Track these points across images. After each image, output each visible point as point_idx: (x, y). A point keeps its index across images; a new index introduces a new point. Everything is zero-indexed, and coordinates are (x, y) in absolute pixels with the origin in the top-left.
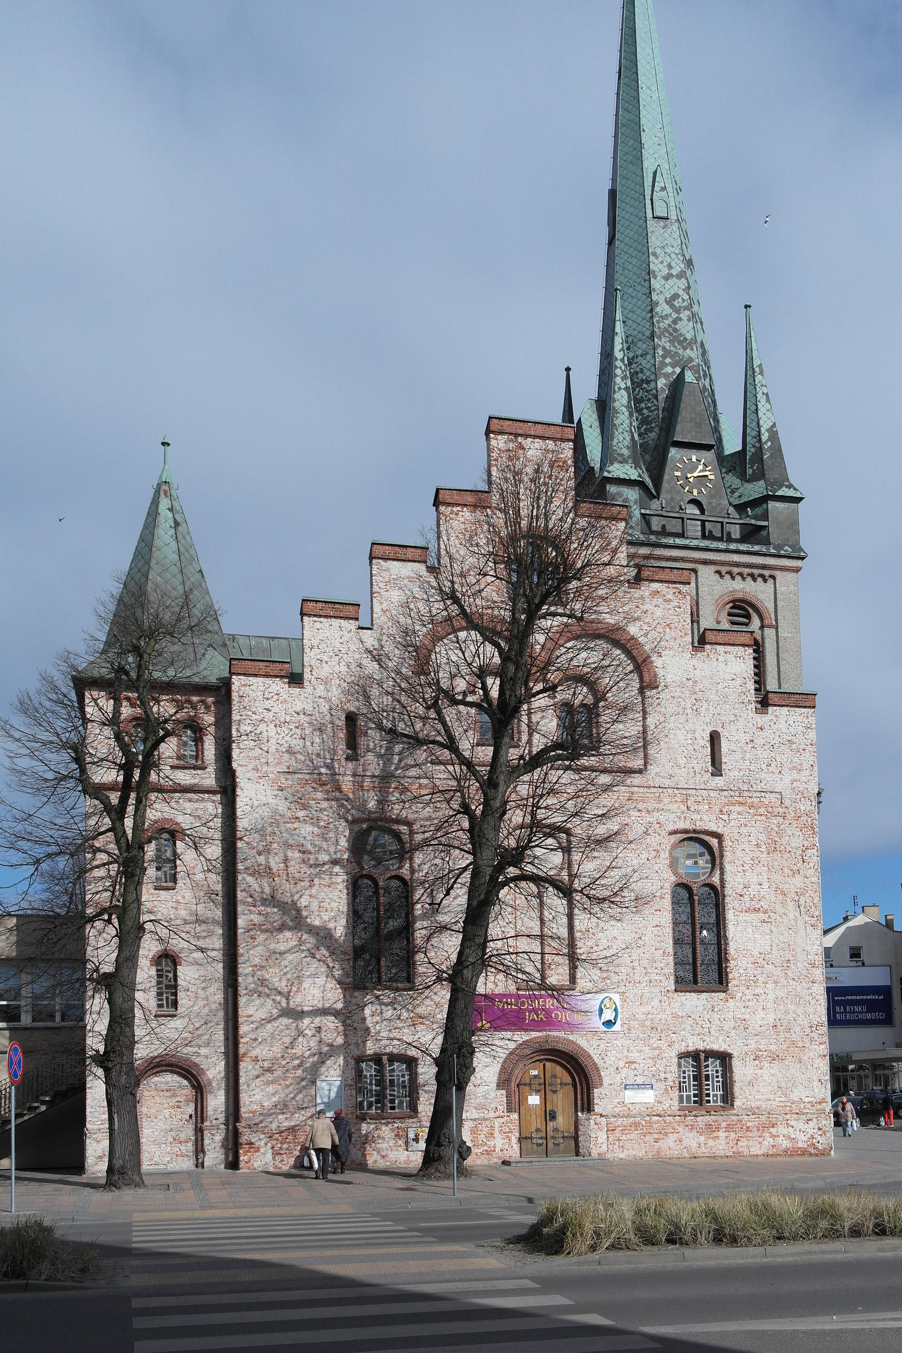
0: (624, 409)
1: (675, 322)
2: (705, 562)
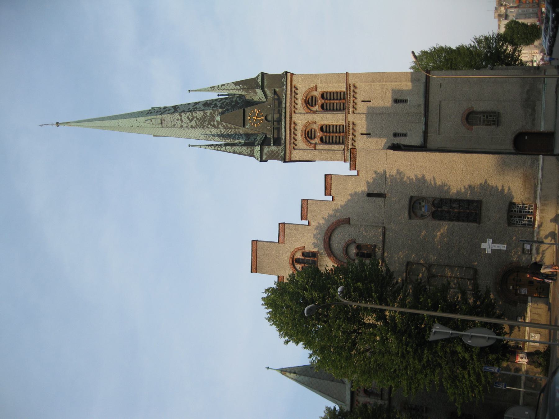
1: (198, 119)
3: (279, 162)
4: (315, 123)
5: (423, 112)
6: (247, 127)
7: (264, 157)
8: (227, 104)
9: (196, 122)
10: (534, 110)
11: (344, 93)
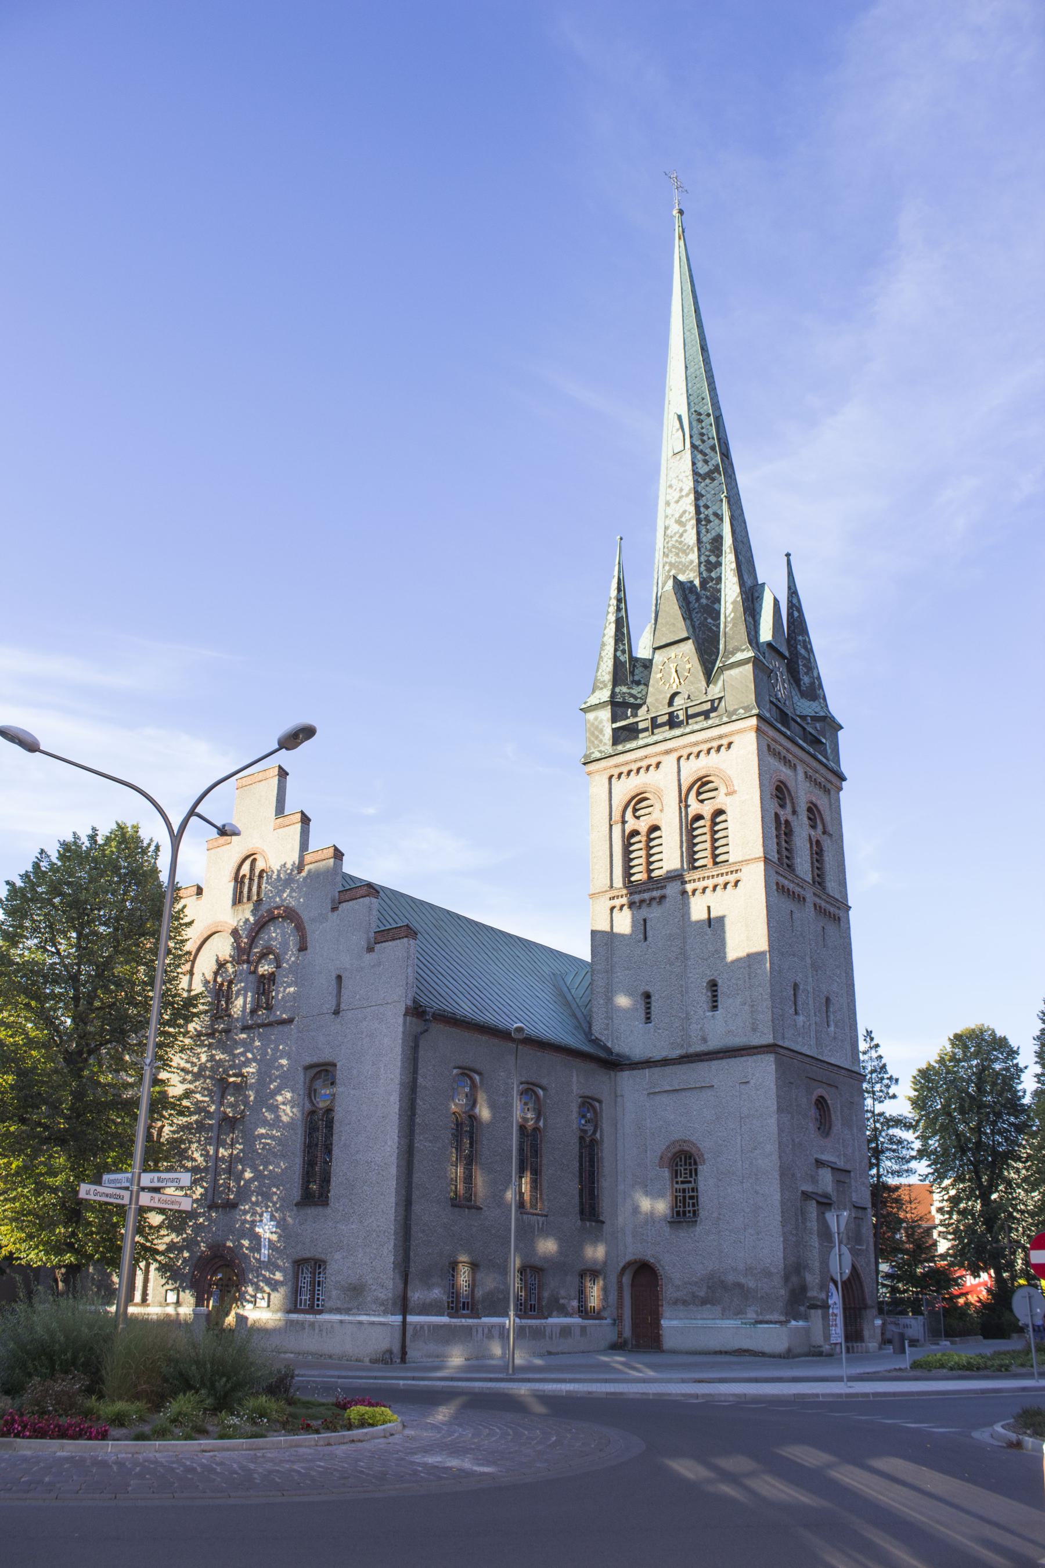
1: (681, 536)
4: (661, 811)
5: (691, 1050)
10: (704, 1302)
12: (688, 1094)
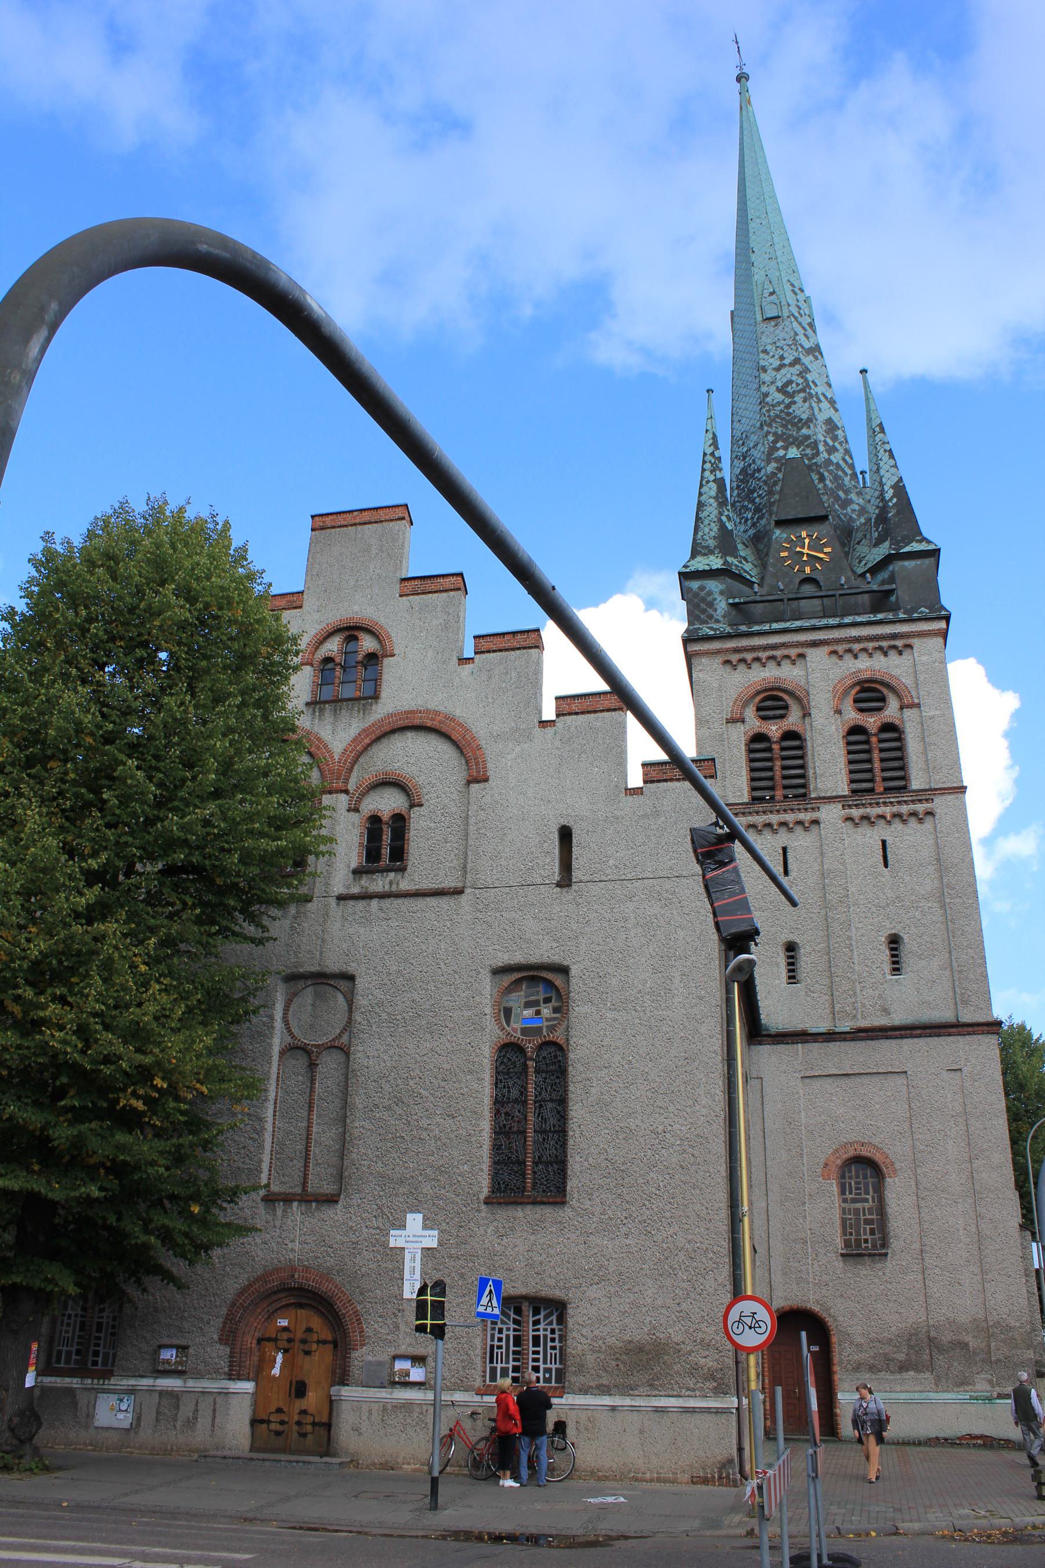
0: (712, 501)
1: (788, 406)
2: (815, 644)
3: (681, 626)
4: (806, 714)
6: (778, 532)
7: (695, 585)
8: (836, 478)
9: (779, 403)
10: (903, 1368)
11: (905, 787)
12: (866, 1080)
